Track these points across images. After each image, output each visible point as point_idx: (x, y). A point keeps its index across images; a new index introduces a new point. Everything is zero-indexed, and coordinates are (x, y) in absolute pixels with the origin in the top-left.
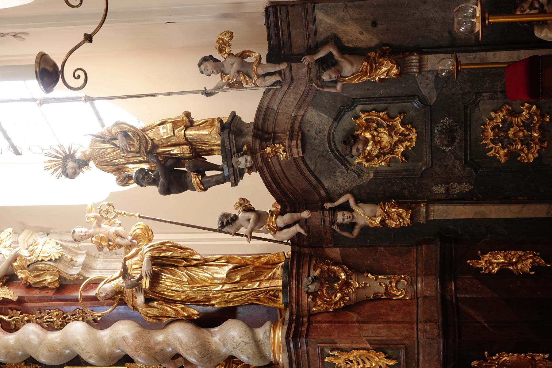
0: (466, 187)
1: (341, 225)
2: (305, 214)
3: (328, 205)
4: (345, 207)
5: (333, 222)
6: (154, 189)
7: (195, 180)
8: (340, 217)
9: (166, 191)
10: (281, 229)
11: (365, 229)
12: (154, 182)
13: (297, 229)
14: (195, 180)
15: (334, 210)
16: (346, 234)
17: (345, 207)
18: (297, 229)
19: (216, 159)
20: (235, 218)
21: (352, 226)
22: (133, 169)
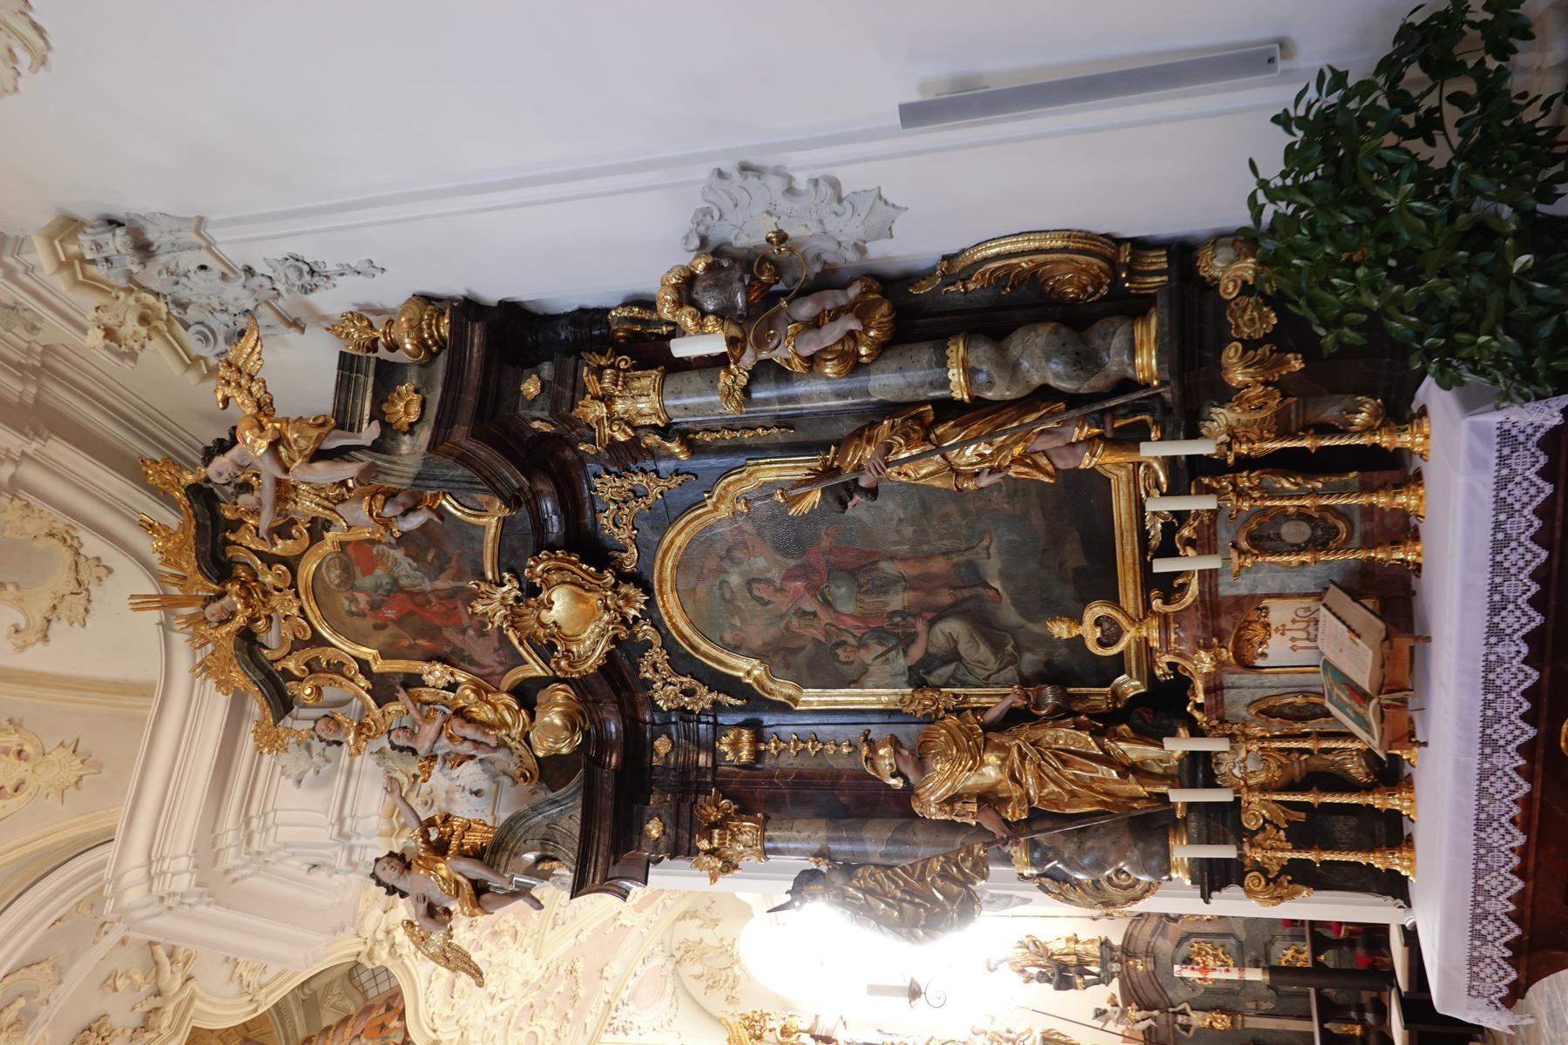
0: (1270, 1005)
1: (1180, 1025)
2: (1156, 1013)
3: (1171, 1010)
4: (1183, 1013)
5: (1175, 1022)
6: (1049, 987)
7: (1079, 981)
8: (1180, 1019)
9: (1058, 988)
10: (1138, 1022)
11: (1200, 1030)
12: (1049, 981)
13: (1150, 1022)
14: (1079, 981)
15: (1175, 1013)
16: (1184, 1033)
17: (1183, 1013)
18: (1150, 1022)
19: (1095, 969)
20: (1105, 1011)
21: (1187, 1028)
22: (1034, 971)
